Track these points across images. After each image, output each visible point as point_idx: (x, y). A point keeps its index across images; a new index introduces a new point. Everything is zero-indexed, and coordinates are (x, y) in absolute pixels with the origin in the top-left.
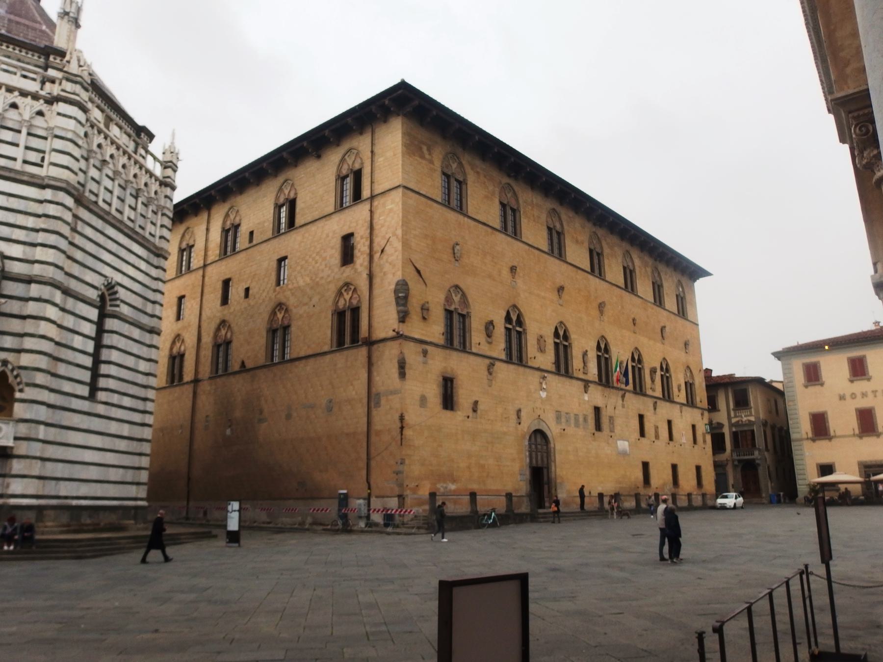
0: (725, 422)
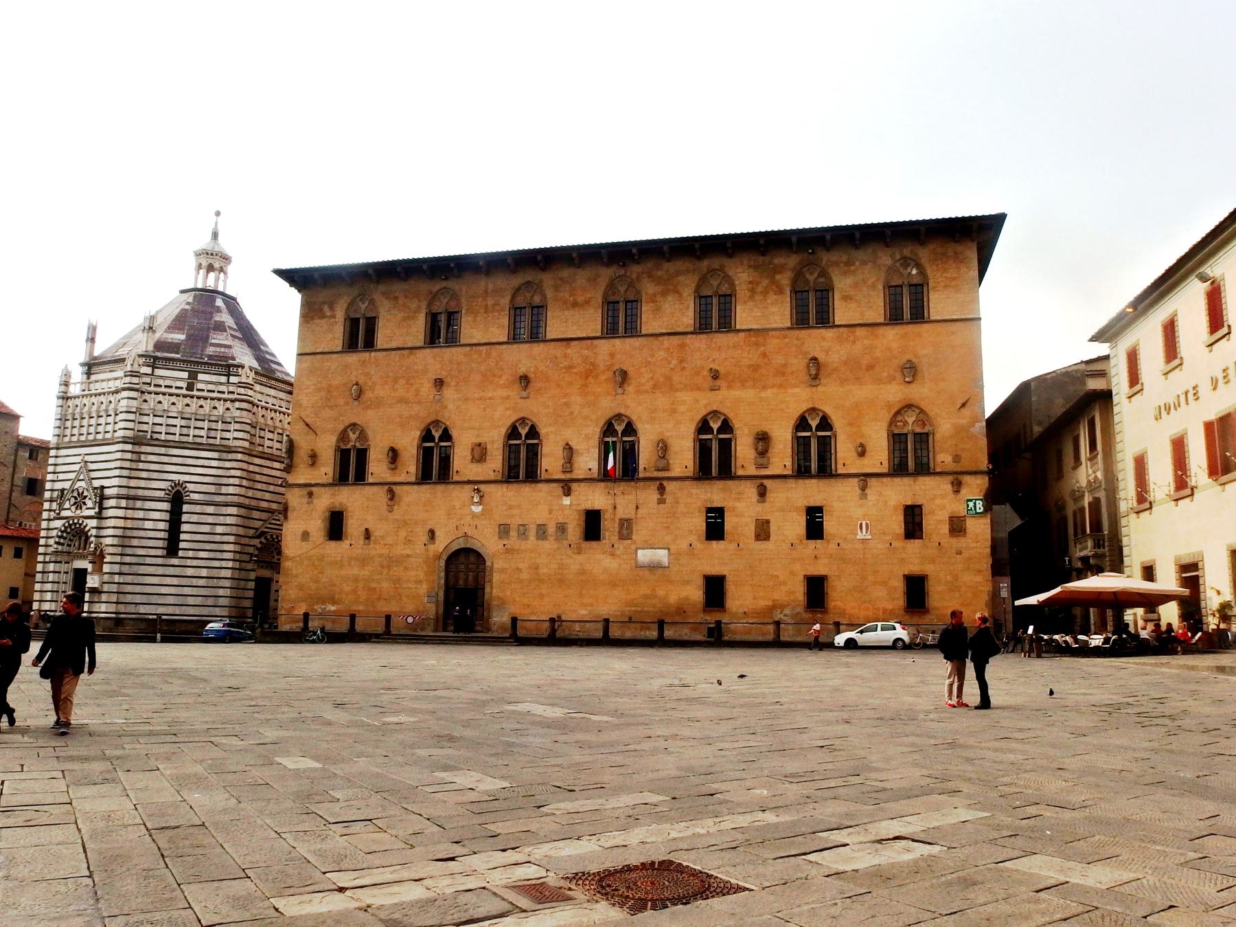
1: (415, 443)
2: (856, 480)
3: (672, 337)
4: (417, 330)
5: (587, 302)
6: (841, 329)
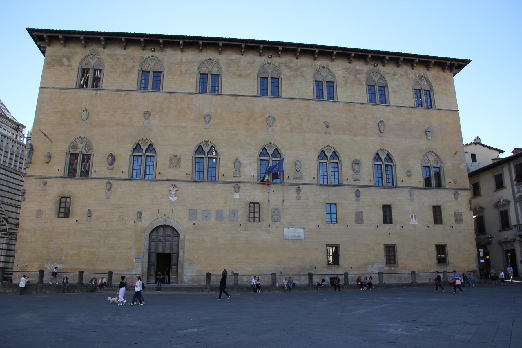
0: (511, 198)
1: (129, 152)
2: (407, 190)
3: (301, 101)
4: (132, 80)
5: (248, 75)
6: (393, 108)
